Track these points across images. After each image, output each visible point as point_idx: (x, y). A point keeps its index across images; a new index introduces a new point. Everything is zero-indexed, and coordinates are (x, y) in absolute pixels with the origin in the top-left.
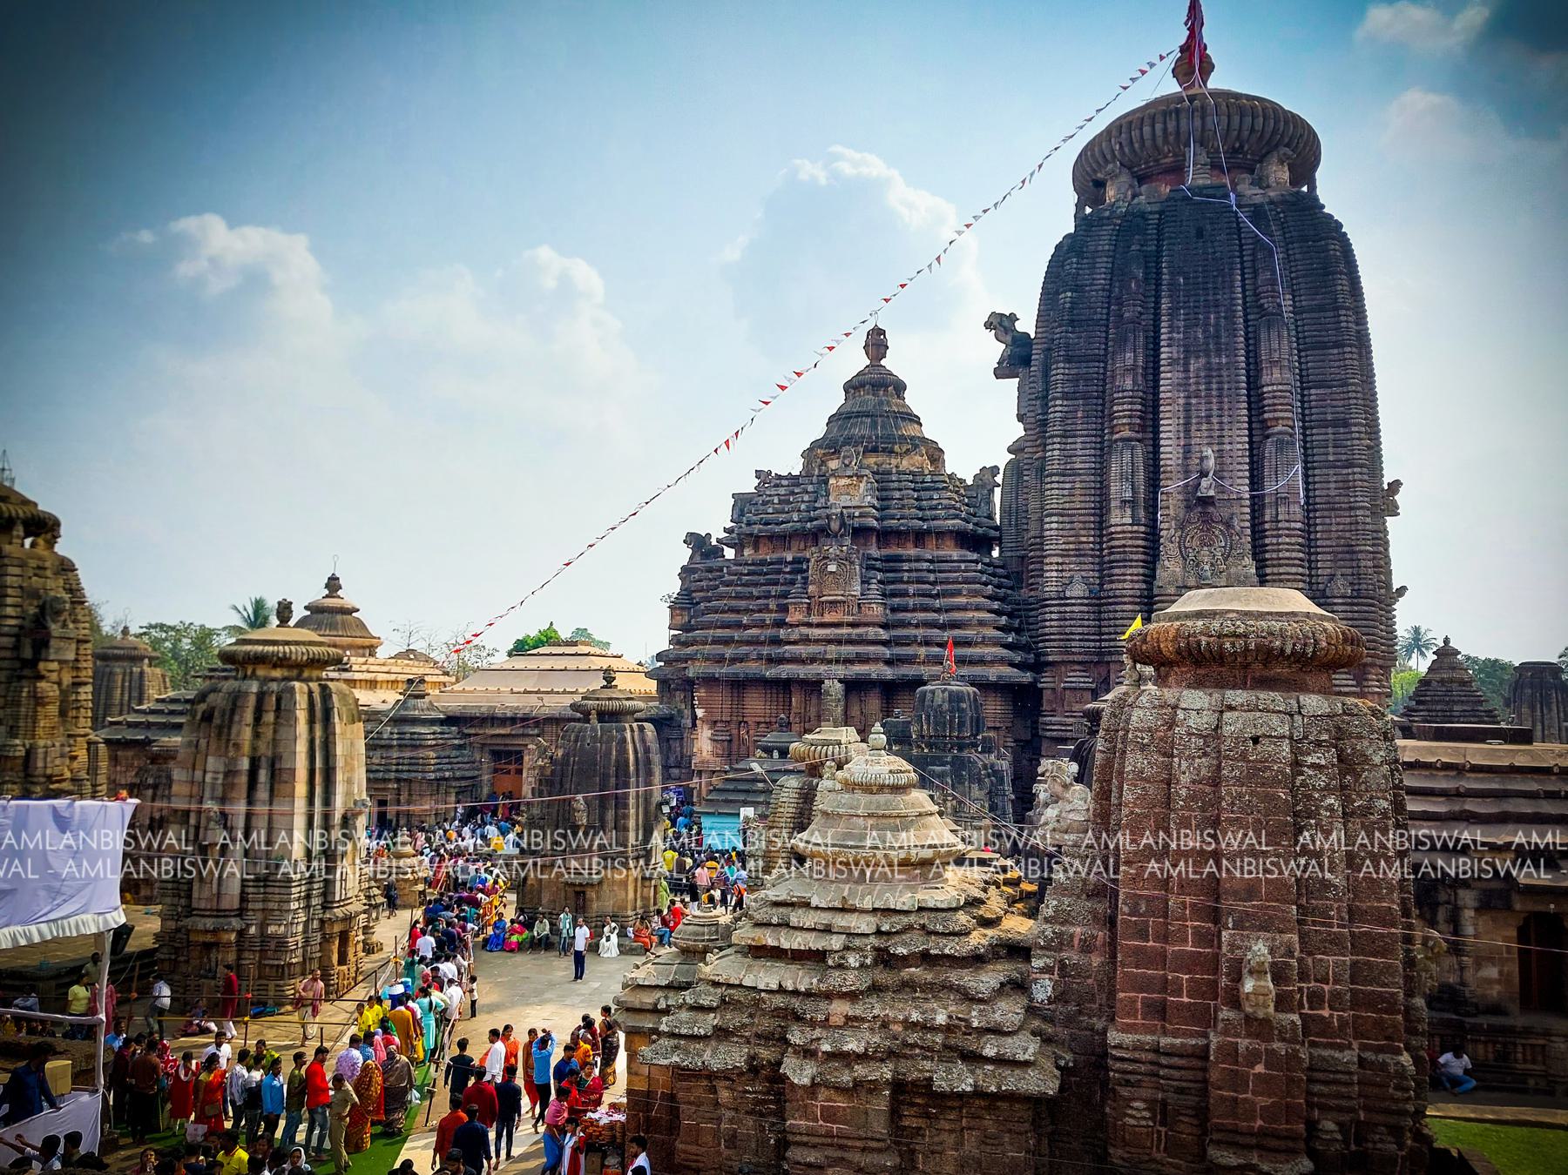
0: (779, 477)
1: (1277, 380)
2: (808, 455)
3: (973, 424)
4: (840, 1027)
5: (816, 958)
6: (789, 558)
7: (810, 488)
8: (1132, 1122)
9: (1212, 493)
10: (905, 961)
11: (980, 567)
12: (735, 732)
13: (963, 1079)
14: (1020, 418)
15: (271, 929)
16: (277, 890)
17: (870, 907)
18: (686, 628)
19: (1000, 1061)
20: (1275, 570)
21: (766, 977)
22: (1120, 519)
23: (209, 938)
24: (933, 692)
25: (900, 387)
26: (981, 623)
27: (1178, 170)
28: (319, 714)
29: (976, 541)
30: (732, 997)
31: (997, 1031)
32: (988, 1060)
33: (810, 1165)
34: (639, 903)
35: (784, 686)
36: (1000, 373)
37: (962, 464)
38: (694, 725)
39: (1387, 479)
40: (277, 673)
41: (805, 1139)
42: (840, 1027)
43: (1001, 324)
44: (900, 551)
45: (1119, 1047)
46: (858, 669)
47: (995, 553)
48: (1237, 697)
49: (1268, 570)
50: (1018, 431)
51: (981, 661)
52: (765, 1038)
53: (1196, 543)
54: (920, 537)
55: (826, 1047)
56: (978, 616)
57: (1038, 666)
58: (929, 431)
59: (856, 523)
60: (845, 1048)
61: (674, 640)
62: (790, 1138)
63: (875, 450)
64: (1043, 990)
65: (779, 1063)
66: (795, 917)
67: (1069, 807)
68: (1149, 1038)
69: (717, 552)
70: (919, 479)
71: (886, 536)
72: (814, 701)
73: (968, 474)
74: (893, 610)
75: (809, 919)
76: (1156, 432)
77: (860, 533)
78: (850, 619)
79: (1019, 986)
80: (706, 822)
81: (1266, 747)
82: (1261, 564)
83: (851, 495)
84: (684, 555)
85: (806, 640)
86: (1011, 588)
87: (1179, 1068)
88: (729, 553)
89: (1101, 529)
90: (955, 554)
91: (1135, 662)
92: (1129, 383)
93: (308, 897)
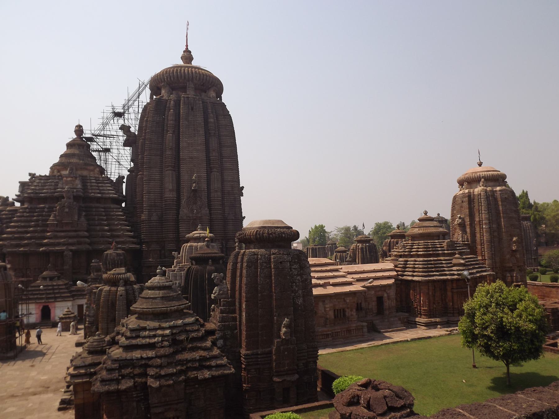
0: (40, 176)
1: (214, 155)
2: (54, 168)
5: (151, 346)
6: (47, 206)
10: (182, 341)
13: (207, 374)
14: (132, 160)
17: (168, 326)
19: (218, 366)
21: (137, 354)
24: (110, 254)
26: (122, 230)
27: (184, 89)
30: (123, 364)
31: (215, 357)
32: (214, 367)
33: (160, 413)
35: (46, 254)
41: (157, 405)
43: (125, 129)
47: (123, 205)
48: (273, 251)
54: (98, 200)
59: (75, 194)
65: (146, 383)
69: (13, 204)
73: (114, 178)
75: (147, 333)
76: (179, 168)
78: (74, 229)
82: (210, 210)
90: (113, 206)
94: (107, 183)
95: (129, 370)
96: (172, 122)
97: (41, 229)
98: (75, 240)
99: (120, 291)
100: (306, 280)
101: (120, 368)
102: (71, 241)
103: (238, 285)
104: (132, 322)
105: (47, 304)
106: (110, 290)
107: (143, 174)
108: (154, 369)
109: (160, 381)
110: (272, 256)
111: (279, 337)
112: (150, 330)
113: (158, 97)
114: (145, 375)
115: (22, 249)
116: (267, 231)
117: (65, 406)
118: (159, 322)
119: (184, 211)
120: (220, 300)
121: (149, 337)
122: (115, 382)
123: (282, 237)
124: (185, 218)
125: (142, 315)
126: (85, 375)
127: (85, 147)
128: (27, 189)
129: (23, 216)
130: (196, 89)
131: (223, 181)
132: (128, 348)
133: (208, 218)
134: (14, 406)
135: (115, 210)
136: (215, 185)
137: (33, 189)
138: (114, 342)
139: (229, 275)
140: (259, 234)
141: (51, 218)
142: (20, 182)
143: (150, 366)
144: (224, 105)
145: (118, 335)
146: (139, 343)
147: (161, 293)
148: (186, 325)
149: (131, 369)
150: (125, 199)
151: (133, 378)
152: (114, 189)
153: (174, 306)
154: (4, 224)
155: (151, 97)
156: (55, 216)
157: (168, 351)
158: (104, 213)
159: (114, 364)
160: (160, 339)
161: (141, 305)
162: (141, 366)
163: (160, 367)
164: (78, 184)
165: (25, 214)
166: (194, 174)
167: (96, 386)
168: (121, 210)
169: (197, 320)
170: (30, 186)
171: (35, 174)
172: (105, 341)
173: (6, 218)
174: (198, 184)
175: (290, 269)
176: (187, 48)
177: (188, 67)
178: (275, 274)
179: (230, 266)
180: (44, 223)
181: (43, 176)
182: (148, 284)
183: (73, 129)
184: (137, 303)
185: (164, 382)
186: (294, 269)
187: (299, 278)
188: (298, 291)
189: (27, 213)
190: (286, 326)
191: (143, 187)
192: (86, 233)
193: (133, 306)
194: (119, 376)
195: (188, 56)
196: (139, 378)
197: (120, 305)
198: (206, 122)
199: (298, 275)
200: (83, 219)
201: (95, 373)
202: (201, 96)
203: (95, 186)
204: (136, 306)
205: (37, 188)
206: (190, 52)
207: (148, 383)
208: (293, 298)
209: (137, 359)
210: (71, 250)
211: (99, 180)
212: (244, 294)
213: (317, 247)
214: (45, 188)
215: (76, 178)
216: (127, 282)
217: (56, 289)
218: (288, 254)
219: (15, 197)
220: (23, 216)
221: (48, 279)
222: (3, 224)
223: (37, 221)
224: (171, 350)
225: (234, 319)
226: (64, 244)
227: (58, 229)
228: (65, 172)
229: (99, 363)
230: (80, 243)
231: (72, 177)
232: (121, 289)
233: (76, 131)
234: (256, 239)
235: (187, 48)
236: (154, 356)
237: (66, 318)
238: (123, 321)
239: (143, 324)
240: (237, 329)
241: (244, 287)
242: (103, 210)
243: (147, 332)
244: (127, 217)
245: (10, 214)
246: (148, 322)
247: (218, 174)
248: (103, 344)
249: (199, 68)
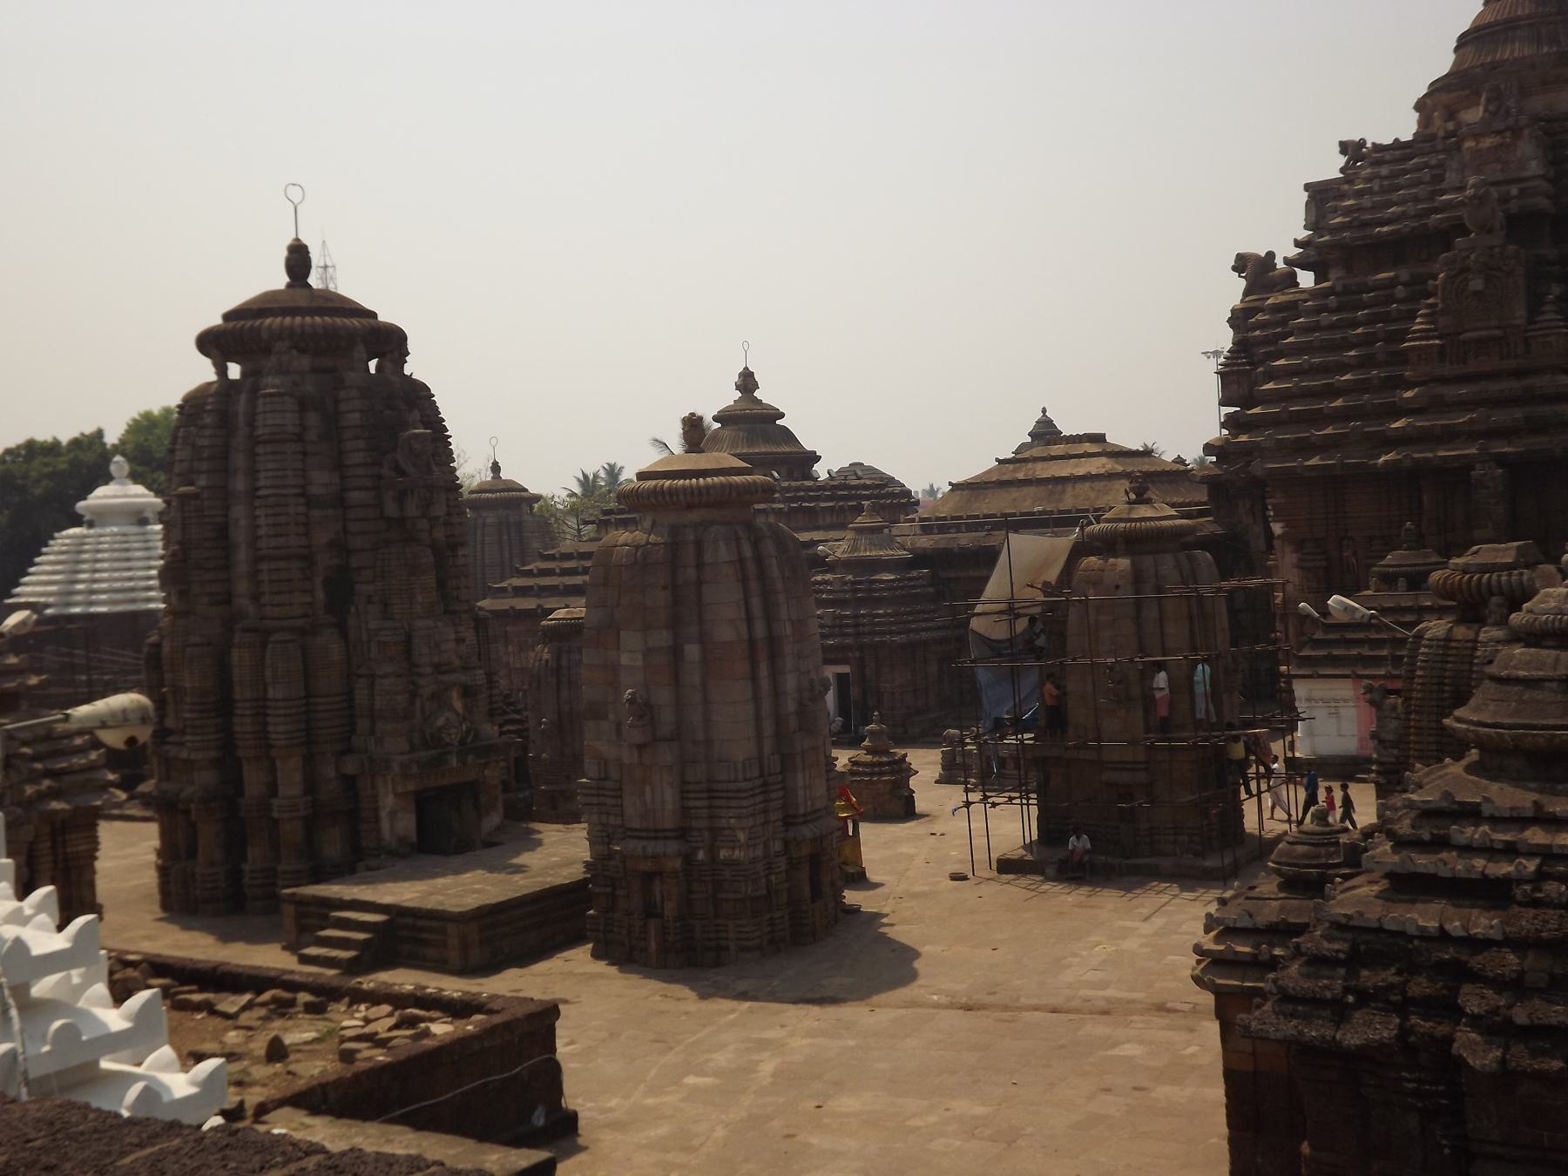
6: (1404, 275)
15: (723, 854)
16: (722, 803)
18: (1246, 402)
21: (1425, 916)
23: (646, 866)
28: (751, 567)
30: (1369, 945)
38: (1270, 547)
40: (694, 516)
52: (1428, 1006)
61: (1229, 423)
65: (1449, 1040)
69: (1291, 280)
80: (1301, 690)
84: (1234, 289)
88: (1306, 279)
93: (765, 811)
95: (1389, 976)
99: (1485, 644)
101: (1354, 961)
102: (1500, 417)
106: (1448, 639)
108: (1489, 993)
109: (1507, 1048)
112: (1496, 821)
114: (1450, 1010)
115: (1314, 461)
118: (1541, 791)
121: (1489, 851)
122: (1327, 1013)
125: (1499, 757)
128: (1335, 210)
132: (1405, 885)
134: (1142, 1042)
137: (1348, 211)
142: (1307, 187)
143: (1475, 977)
146: (1445, 873)
149: (1399, 973)
151: (1404, 1007)
154: (1261, 362)
159: (1330, 939)
160: (1531, 866)
161: (1477, 710)
162: (1440, 967)
163: (1516, 986)
170: (1343, 196)
171: (1362, 143)
172: (1337, 843)
173: (1267, 341)
184: (1472, 702)
185: (1521, 1058)
189: (1332, 311)
193: (1457, 713)
194: (1347, 990)
196: (1426, 1018)
201: (1274, 964)
205: (1366, 201)
207: (1455, 1045)
209: (1424, 936)
219: (1294, 252)
221: (1402, 582)
222: (1254, 365)
223: (1368, 341)
226: (1472, 436)
228: (1474, 115)
236: (1496, 935)
239: (1473, 790)
243: (1485, 828)
245: (1277, 324)
246: (1495, 788)
248: (1330, 855)
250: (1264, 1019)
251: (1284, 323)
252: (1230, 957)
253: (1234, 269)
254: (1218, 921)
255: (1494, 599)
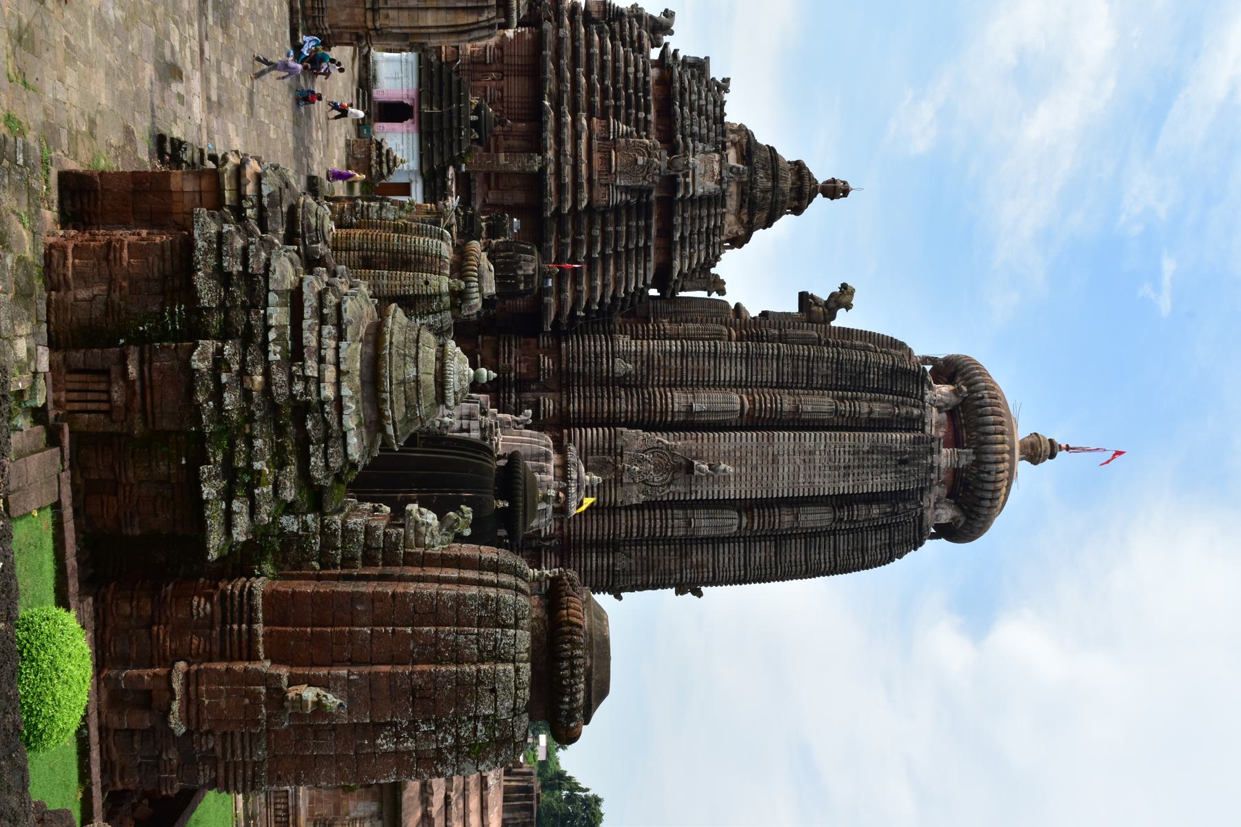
0: (723, 104)
3: (759, 275)
4: (242, 385)
5: (296, 353)
7: (712, 134)
8: (195, 603)
9: (696, 472)
10: (301, 424)
11: (640, 285)
12: (494, 67)
14: (764, 314)
17: (343, 393)
18: (587, 12)
19: (229, 515)
20: (635, 517)
21: (278, 315)
22: (679, 400)
25: (798, 211)
26: (592, 289)
27: (955, 441)
29: (663, 279)
34: (336, 31)
35: (535, 115)
36: (804, 298)
37: (729, 265)
39: (703, 589)
42: (242, 385)
43: (843, 297)
44: (654, 218)
45: (250, 593)
46: (551, 183)
47: (653, 292)
48: (526, 668)
49: (635, 513)
50: (754, 311)
51: (560, 290)
53: (657, 460)
54: (666, 232)
55: (224, 378)
56: (600, 287)
57: (559, 333)
58: (758, 235)
59: (681, 179)
60: (225, 395)
61: (575, 6)
62: (147, 346)
63: (742, 194)
64: (291, 524)
66: (328, 329)
67: (436, 533)
68: (260, 615)
69: (656, 44)
70: (717, 232)
71: (668, 205)
72: (522, 143)
73: (718, 270)
74: (603, 214)
77: (670, 183)
78: (596, 177)
79: (289, 508)
80: (411, 57)
81: (488, 698)
82: (640, 507)
83: (704, 171)
85: (576, 137)
86: (622, 308)
87: (240, 641)
88: (655, 54)
89: (670, 386)
90: (652, 265)
91: (552, 580)
92: (786, 407)
94: (708, 254)
96: (865, 410)
97: (598, 105)
98: (568, 180)
100: (444, 762)
102: (568, 169)
103: (436, 572)
104: (358, 305)
105: (416, 115)
107: (730, 339)
110: (510, 667)
111: (294, 681)
113: (930, 378)
114: (224, 336)
116: (579, 652)
117: (169, 151)
119: (635, 438)
120: (402, 526)
123: (563, 695)
124: (619, 443)
126: (240, 195)
127: (796, 203)
128: (692, 75)
129: (627, 65)
130: (956, 472)
131: (715, 541)
133: (619, 500)
135: (641, 272)
136: (704, 524)
138: (310, 263)
139: (467, 550)
140: (571, 633)
141: (623, 128)
142: (707, 58)
144: (917, 544)
145: (328, 271)
147: (429, 379)
148: (344, 436)
150: (668, 296)
151: (222, 306)
152: (694, 271)
153: (392, 408)
155: (926, 360)
156: (628, 135)
157: (280, 392)
158: (631, 246)
162: (249, 326)
164: (704, 185)
165: (631, 69)
166: (735, 466)
167: (208, 219)
168: (640, 285)
169: (354, 466)
171: (727, 91)
172: (318, 242)
174: (708, 475)
175: (476, 718)
176: (1061, 448)
177: (1011, 452)
178: (463, 673)
179: (488, 553)
180: (611, 111)
181: (722, 110)
182: (451, 345)
183: (839, 177)
184: (405, 320)
186: (475, 729)
187: (450, 740)
188: (415, 737)
190: (318, 704)
191: (698, 340)
192: (584, 204)
193: (400, 313)
195: (1039, 451)
197: (406, 281)
198: (871, 498)
199: (457, 737)
200: (619, 197)
202: (939, 484)
203: (701, 227)
204: (397, 317)
205: (694, 97)
206: (1052, 456)
208: (395, 724)
210: (543, 170)
211: (714, 235)
212: (412, 588)
213: (534, 802)
214: (695, 113)
215: (720, 182)
216: (460, 297)
217: (451, 135)
218: (514, 710)
219: (671, 49)
220: (627, 65)
224: (280, 400)
225: (348, 561)
226: (559, 153)
227: (595, 142)
229: (264, 230)
230: (560, 187)
231: (721, 173)
232: (443, 283)
233: (834, 181)
234: (561, 625)
235: (1061, 448)
236: (271, 357)
237: (380, 155)
238: (363, 287)
240: (322, 568)
241: (431, 589)
242: (641, 244)
244: (624, 300)
247: (735, 529)
248: (310, 238)
249: (1010, 480)
250: (206, 227)
251: (632, 42)
252: (243, 181)
253: (666, 10)
254: (265, 174)
255: (463, 283)
